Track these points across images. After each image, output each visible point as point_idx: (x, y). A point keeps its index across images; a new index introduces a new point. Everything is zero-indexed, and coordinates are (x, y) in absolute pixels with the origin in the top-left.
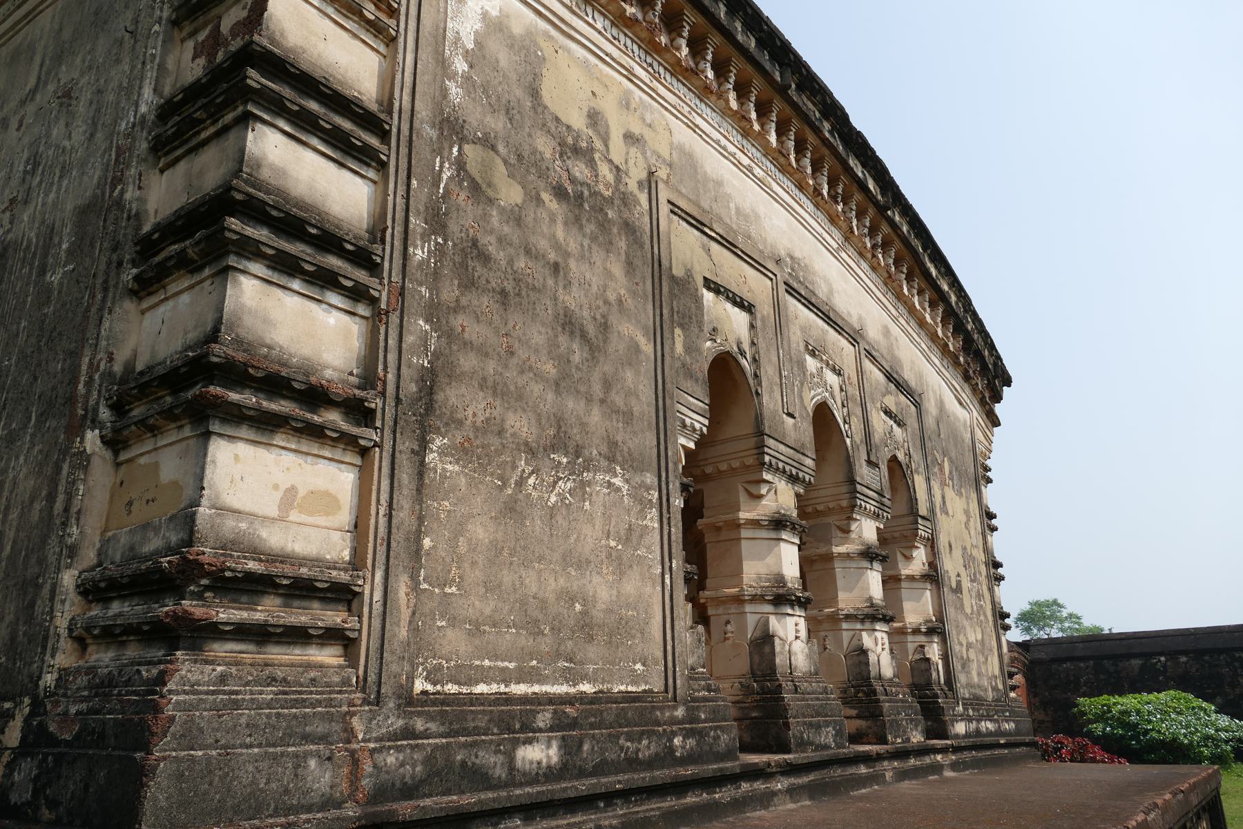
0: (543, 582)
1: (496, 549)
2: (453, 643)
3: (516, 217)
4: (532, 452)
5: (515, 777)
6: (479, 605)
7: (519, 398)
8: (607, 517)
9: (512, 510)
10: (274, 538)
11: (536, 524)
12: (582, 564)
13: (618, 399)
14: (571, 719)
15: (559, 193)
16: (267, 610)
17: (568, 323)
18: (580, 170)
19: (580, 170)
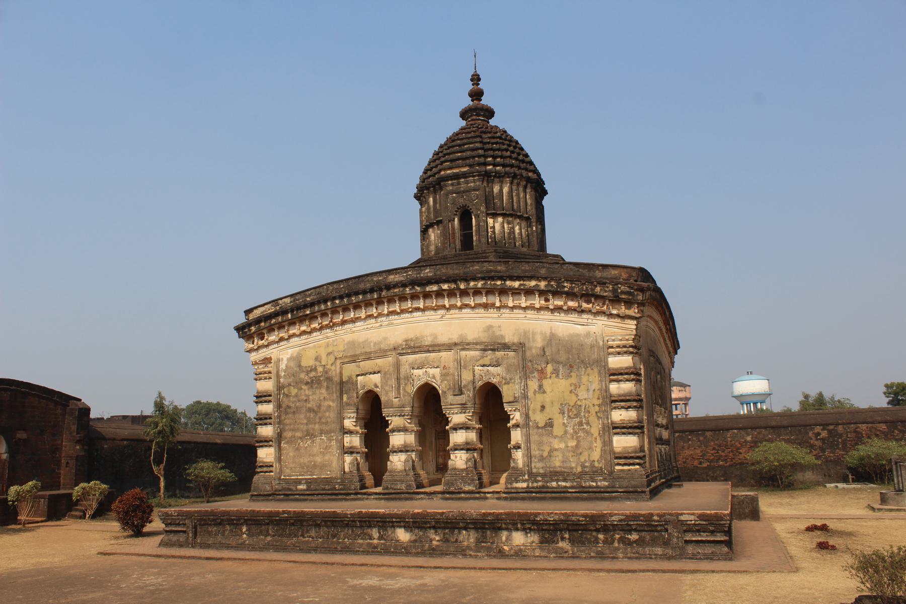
0: (305, 460)
1: (294, 456)
2: (288, 471)
3: (296, 396)
4: (301, 438)
5: (297, 490)
6: (292, 465)
7: (298, 430)
8: (320, 445)
9: (298, 449)
10: (265, 460)
11: (302, 451)
12: (313, 455)
13: (324, 420)
14: (308, 482)
15: (307, 383)
16: (265, 469)
17: (310, 410)
18: (313, 374)
19: (313, 374)
